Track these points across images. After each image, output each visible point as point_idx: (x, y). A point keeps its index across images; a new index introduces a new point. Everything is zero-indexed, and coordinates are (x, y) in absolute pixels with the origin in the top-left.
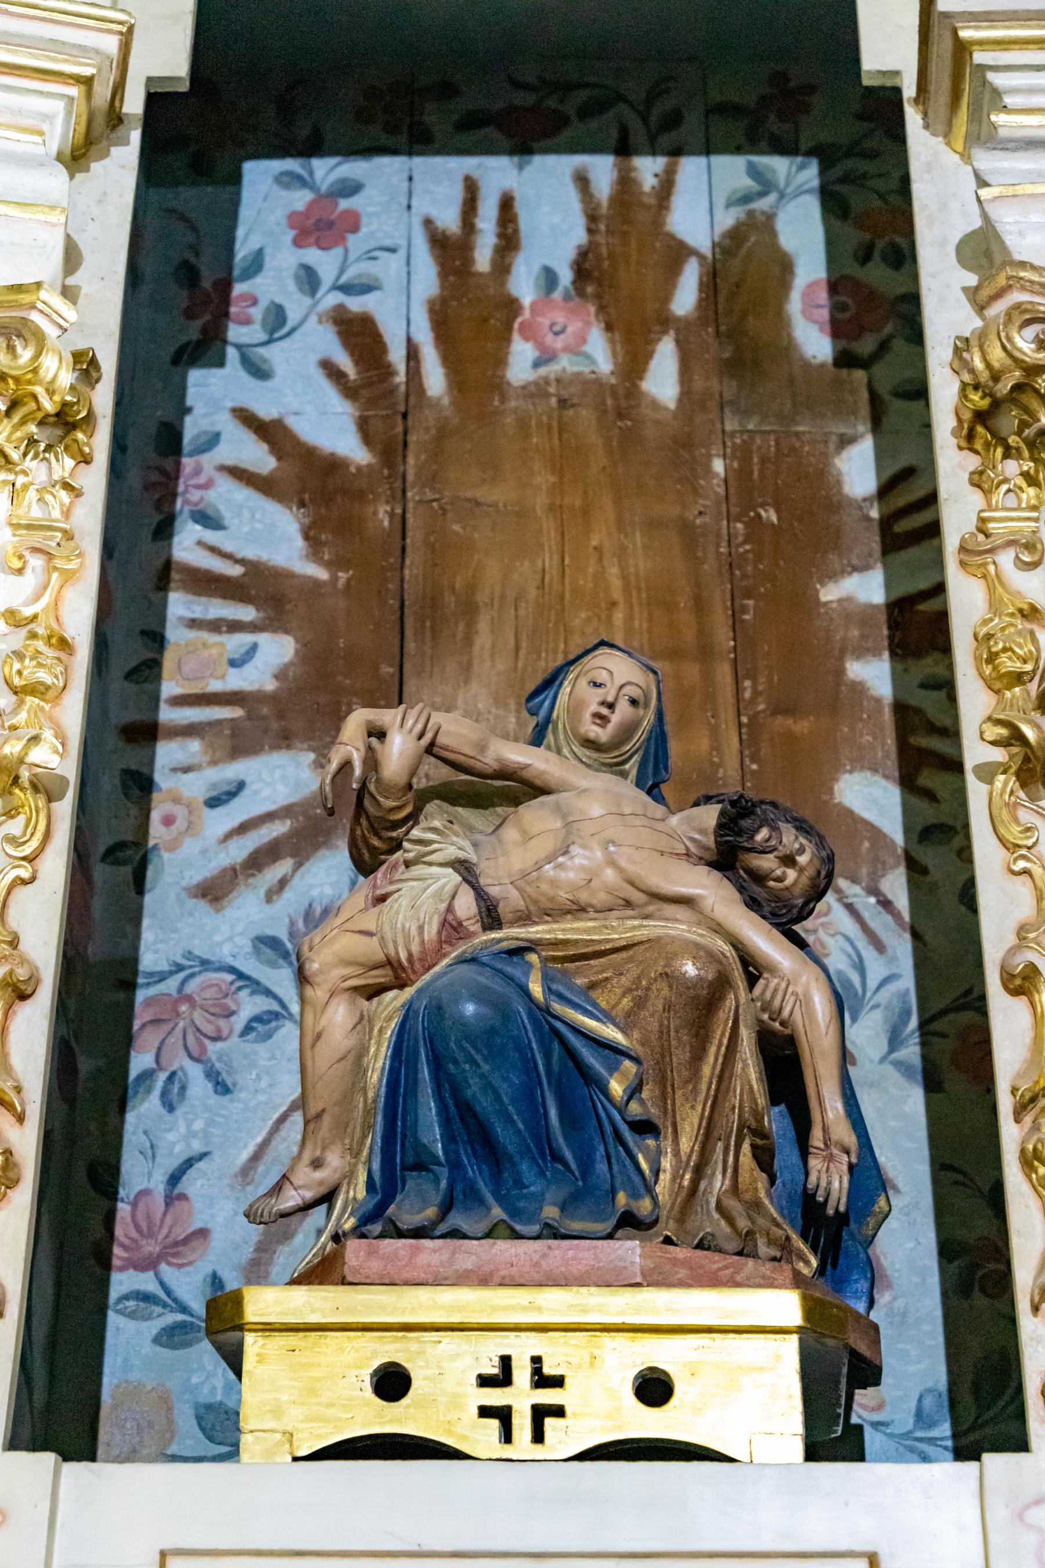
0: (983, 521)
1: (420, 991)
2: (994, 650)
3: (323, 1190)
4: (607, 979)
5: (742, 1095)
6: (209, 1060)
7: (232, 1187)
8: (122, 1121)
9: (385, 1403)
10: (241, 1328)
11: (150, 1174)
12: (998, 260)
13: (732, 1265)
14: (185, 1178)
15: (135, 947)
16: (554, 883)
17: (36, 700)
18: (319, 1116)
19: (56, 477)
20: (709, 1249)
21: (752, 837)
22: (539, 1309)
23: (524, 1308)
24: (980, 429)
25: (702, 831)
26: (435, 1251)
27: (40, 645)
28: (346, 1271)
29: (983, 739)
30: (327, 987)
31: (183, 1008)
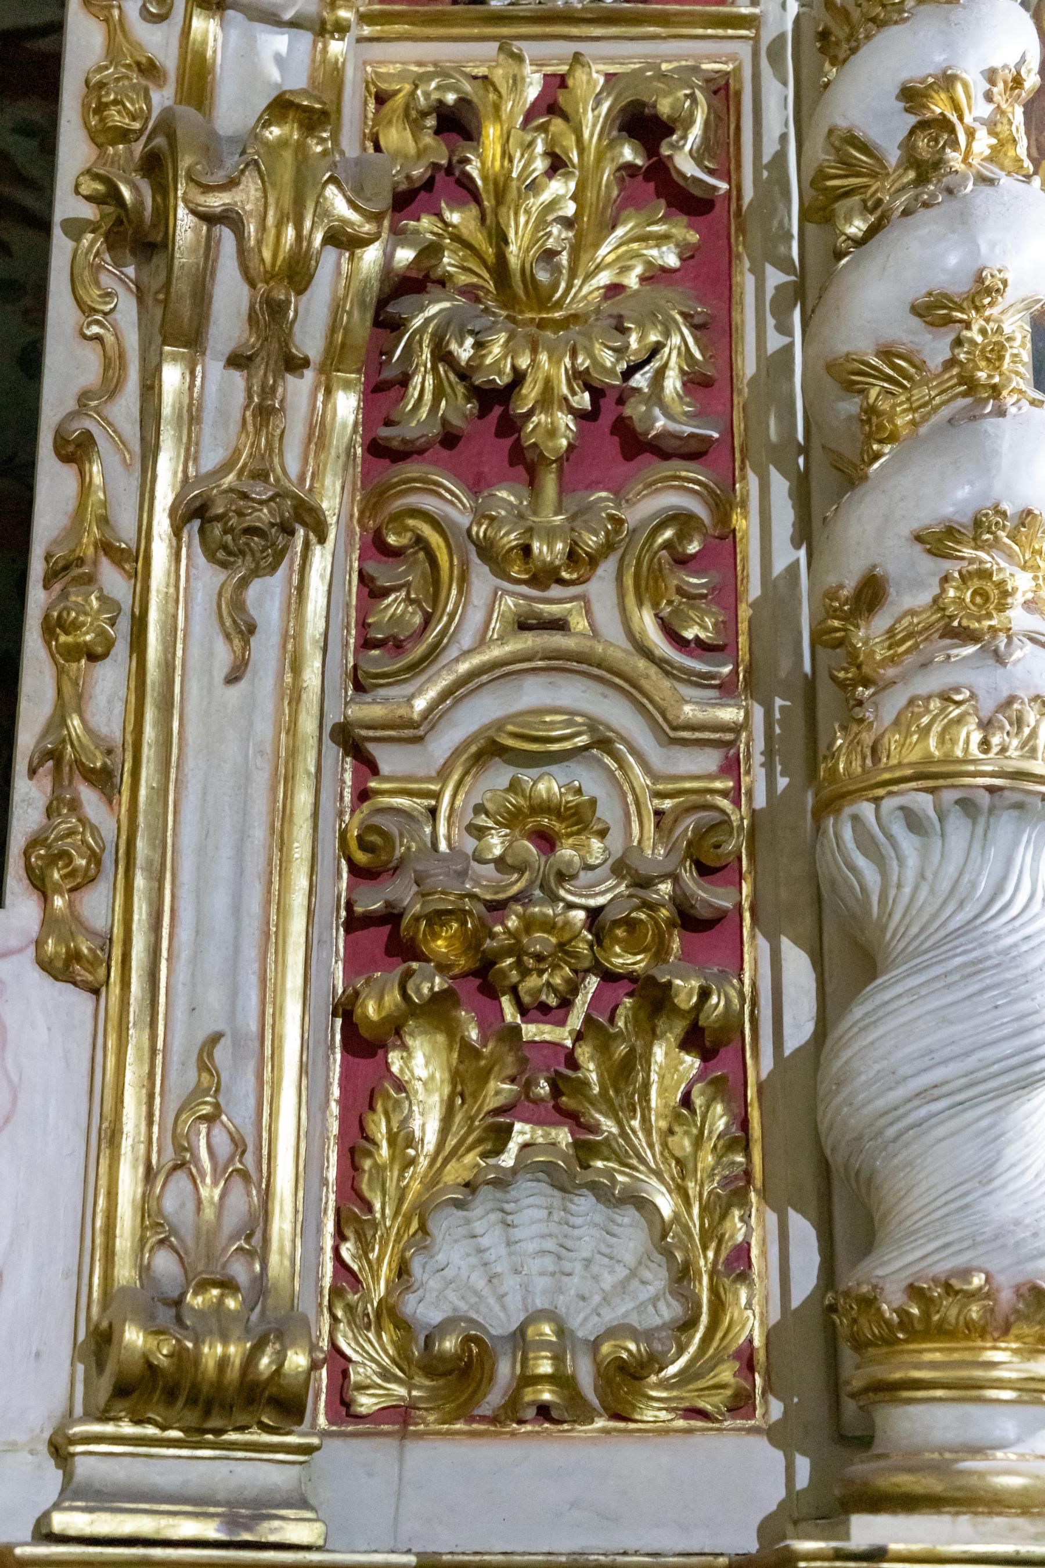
2: (104, 100)
29: (77, 193)
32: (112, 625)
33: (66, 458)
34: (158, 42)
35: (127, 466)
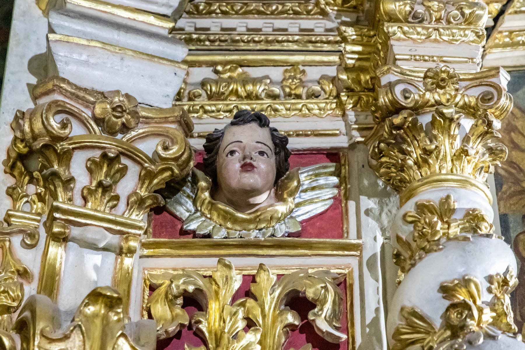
0: (9, 216)
12: (51, 74)
24: (19, 164)
34: (30, 259)
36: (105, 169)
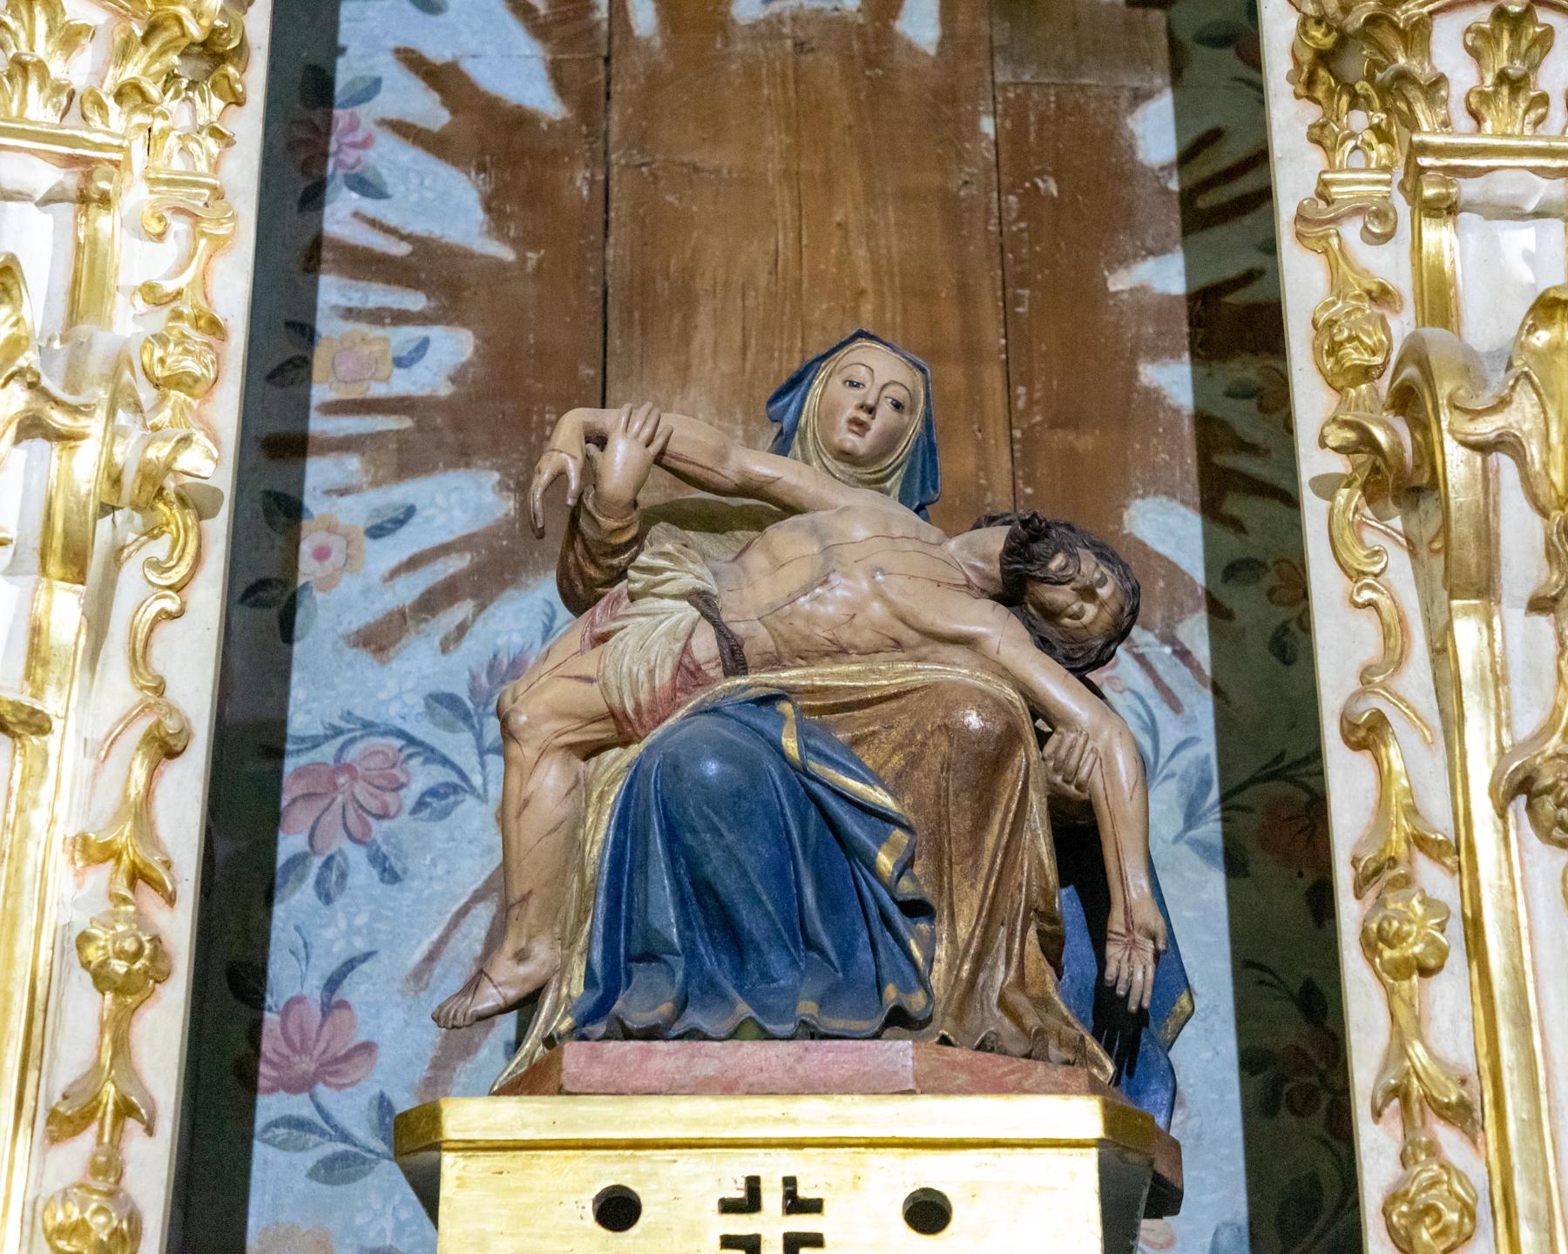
1: (649, 748)
2: (1337, 338)
3: (528, 988)
4: (873, 733)
5: (1029, 871)
6: (374, 841)
7: (403, 993)
8: (269, 915)
9: (610, 1233)
10: (437, 1147)
11: (303, 979)
13: (1019, 1069)
14: (346, 982)
15: (283, 708)
16: (810, 619)
17: (182, 395)
18: (524, 899)
19: (201, 121)
20: (992, 1050)
21: (1045, 565)
22: (794, 1121)
23: (777, 1121)
24: (1322, 73)
25: (986, 558)
26: (668, 1054)
27: (185, 327)
28: (564, 1078)
30: (537, 743)
31: (342, 780)
32: (1442, 931)
33: (1358, 746)
34: (1387, 264)
35: (1430, 746)
36: (1506, 42)
